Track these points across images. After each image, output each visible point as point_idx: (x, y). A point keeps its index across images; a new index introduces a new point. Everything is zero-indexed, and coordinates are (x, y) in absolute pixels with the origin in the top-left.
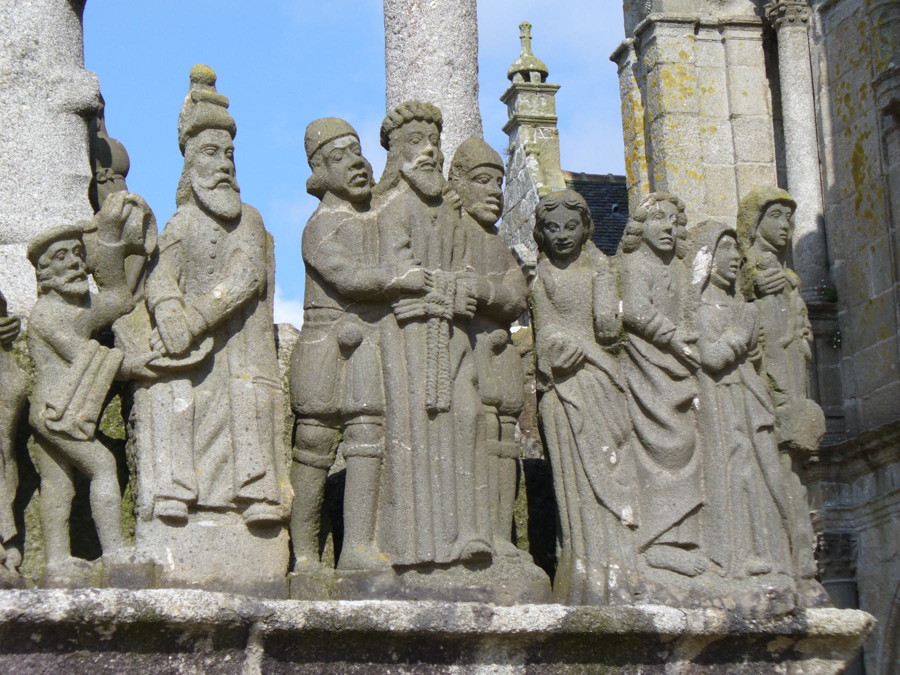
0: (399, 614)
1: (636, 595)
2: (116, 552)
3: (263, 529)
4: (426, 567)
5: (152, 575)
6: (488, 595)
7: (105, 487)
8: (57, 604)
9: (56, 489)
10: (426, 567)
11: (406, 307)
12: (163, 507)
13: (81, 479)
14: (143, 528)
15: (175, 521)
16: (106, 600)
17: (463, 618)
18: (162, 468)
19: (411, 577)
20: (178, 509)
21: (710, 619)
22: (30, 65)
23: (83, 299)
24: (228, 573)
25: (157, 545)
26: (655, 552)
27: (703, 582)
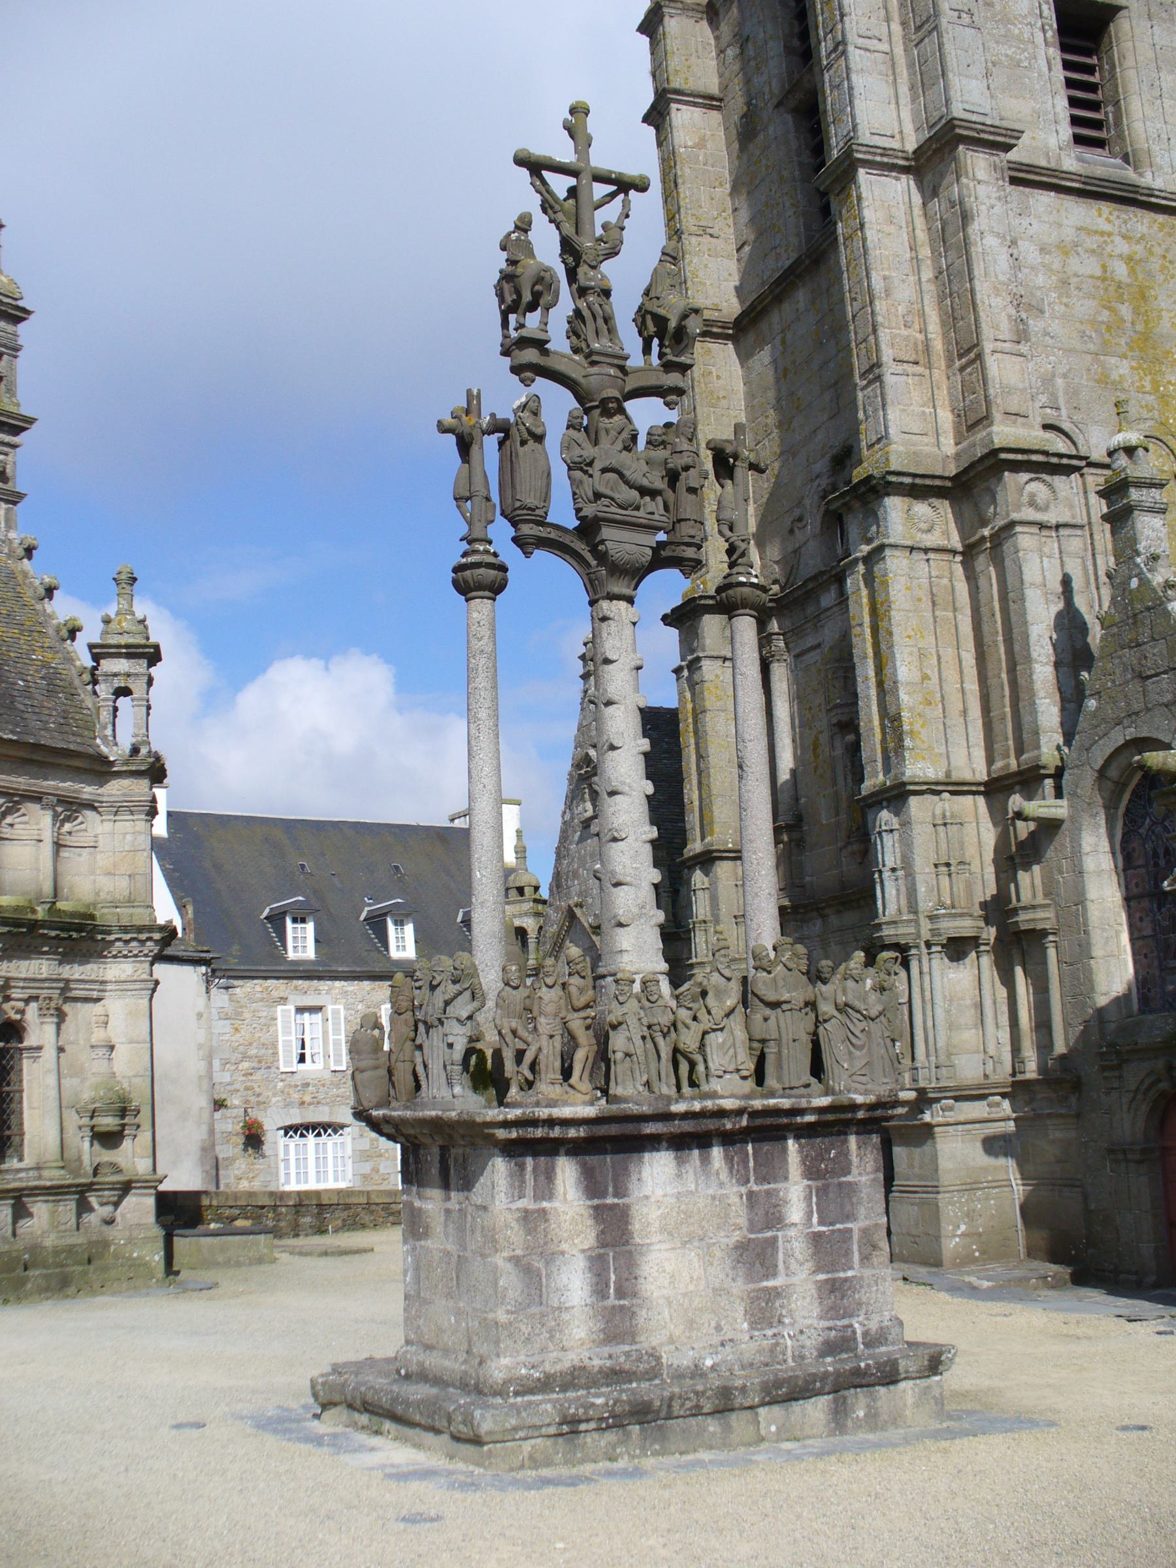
0: (785, 1103)
1: (849, 1091)
2: (705, 1087)
3: (744, 1078)
4: (792, 1088)
5: (713, 1095)
6: (810, 1096)
7: (701, 1068)
8: (697, 1106)
9: (684, 1067)
10: (792, 1088)
11: (785, 1007)
12: (717, 1073)
13: (692, 1065)
14: (711, 1079)
15: (720, 1077)
16: (709, 1104)
17: (803, 1103)
18: (716, 1061)
19: (787, 1091)
20: (721, 1073)
21: (872, 1098)
22: (644, 911)
23: (690, 1009)
24: (735, 1092)
25: (716, 1085)
26: (855, 1078)
27: (869, 1087)
